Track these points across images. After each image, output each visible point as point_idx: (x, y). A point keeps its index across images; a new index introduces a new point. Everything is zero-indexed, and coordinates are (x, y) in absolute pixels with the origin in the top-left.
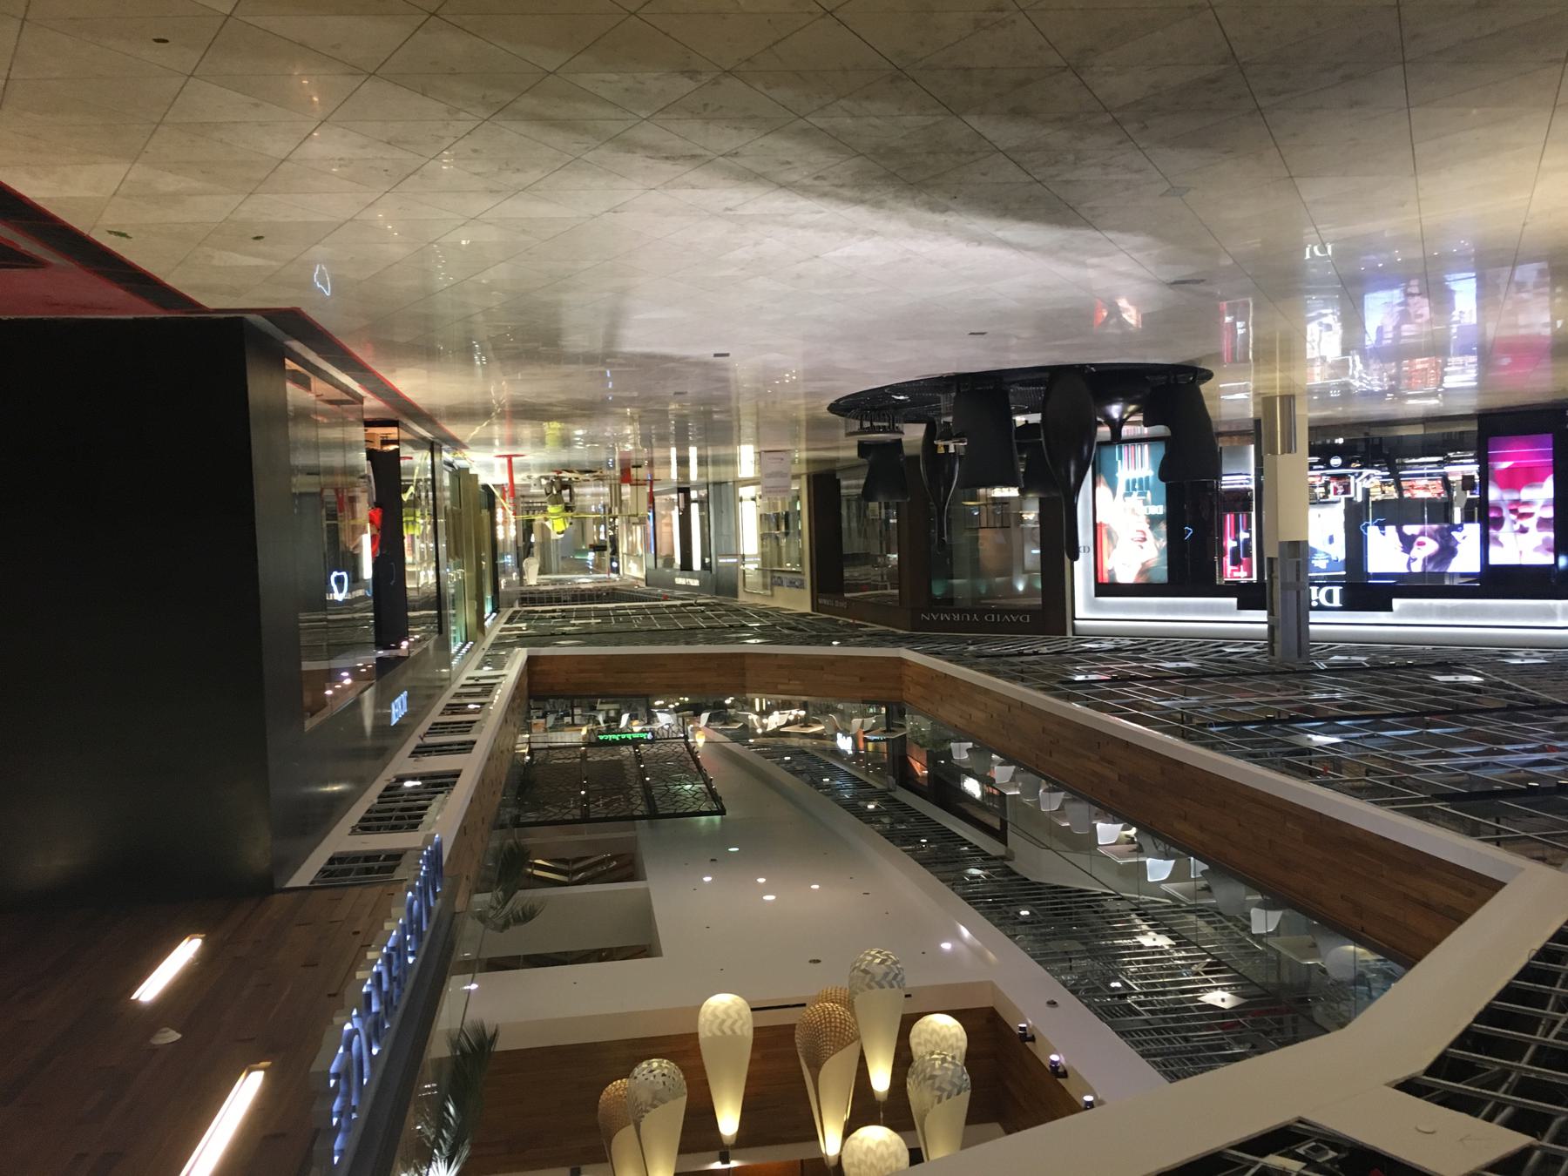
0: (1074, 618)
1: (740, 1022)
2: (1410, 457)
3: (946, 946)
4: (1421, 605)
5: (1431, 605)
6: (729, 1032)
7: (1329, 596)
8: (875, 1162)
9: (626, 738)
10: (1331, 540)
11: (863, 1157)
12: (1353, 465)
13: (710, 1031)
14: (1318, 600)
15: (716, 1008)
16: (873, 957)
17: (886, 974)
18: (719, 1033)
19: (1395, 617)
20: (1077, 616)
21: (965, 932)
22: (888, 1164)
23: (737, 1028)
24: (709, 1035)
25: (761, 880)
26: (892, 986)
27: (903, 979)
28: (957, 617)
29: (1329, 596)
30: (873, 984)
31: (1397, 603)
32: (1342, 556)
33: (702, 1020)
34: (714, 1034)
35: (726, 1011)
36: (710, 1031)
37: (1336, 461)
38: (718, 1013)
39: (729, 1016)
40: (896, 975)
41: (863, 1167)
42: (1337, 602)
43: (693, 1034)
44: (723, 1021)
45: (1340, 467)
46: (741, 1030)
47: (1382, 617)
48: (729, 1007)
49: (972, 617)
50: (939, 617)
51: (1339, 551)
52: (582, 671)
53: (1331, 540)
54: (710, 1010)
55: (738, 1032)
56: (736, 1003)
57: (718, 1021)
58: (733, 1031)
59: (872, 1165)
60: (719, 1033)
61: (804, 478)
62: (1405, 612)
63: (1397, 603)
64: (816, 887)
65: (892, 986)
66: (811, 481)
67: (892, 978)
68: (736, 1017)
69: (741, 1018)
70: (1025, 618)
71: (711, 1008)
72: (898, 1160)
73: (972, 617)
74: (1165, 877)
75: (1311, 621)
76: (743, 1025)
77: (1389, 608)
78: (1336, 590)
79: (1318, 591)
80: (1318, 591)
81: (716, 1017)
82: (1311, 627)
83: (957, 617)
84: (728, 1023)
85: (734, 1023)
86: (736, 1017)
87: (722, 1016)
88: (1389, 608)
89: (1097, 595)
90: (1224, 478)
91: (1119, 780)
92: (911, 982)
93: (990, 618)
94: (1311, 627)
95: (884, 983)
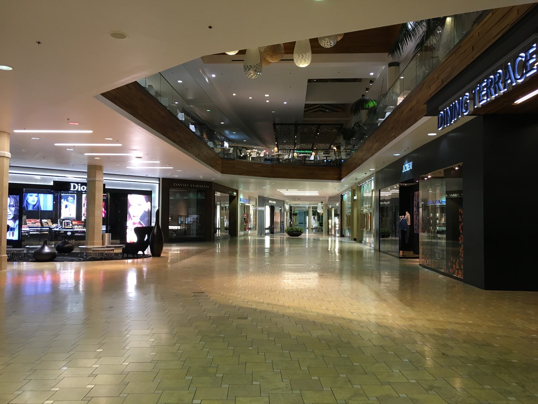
0: (159, 184)
1: (296, 58)
2: (38, 234)
3: (214, 76)
4: (43, 183)
5: (40, 182)
6: (300, 55)
7: (74, 187)
9: (303, 151)
10: (66, 207)
12: (63, 232)
14: (78, 186)
15: (304, 63)
16: (252, 74)
17: (249, 70)
18: (304, 54)
19: (52, 178)
20: (158, 184)
21: (207, 80)
23: (298, 56)
24: (307, 54)
25: (268, 101)
26: (247, 66)
27: (244, 69)
28: (197, 186)
29: (74, 187)
30: (253, 67)
31: (52, 184)
32: (62, 200)
33: (310, 59)
35: (301, 61)
36: (306, 55)
37: (69, 234)
38: (304, 61)
39: (300, 60)
40: (246, 70)
42: (72, 184)
43: (313, 53)
44: (302, 58)
45: (68, 231)
47: (57, 179)
48: (300, 63)
49: (193, 186)
50: (203, 186)
51: (64, 203)
53: (66, 207)
54: (307, 62)
55: (297, 55)
56: (298, 64)
57: (303, 58)
58: (299, 55)
61: (238, 236)
62: (49, 180)
63: (52, 184)
64: (250, 98)
65: (247, 66)
66: (237, 235)
67: (247, 68)
68: (298, 60)
69: (296, 59)
70: (175, 184)
71: (306, 62)
73: (193, 186)
74: (387, 113)
75: (86, 179)
76: (296, 57)
77: (55, 182)
78: (72, 189)
79: (78, 189)
80: (78, 189)
81: (304, 60)
82: (86, 177)
83: (197, 186)
84: (300, 58)
85: (298, 58)
86: (298, 60)
87: (302, 60)
88: (54, 182)
89: (151, 191)
90: (105, 229)
91: (176, 130)
92: (241, 65)
93: (187, 185)
94: (86, 177)
95: (250, 67)
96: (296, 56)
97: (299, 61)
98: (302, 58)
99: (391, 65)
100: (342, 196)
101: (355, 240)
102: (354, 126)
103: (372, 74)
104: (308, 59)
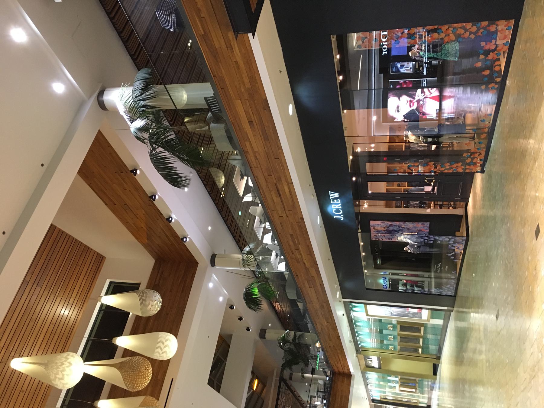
1: (161, 352)
8: (63, 366)
11: (68, 361)
13: (161, 337)
18: (159, 341)
22: (60, 373)
23: (159, 350)
34: (159, 338)
41: (64, 359)
44: (163, 343)
46: (157, 352)
52: (342, 397)
55: (156, 350)
57: (164, 341)
58: (157, 348)
59: (63, 364)
60: (159, 341)
69: (163, 353)
72: (60, 379)
81: (166, 341)
84: (162, 346)
85: (161, 350)
87: (166, 343)
96: (157, 354)
97: (166, 349)
98: (163, 343)
99: (213, 264)
100: (373, 401)
101: (435, 373)
102: (283, 349)
103: (221, 299)
104: (166, 336)
